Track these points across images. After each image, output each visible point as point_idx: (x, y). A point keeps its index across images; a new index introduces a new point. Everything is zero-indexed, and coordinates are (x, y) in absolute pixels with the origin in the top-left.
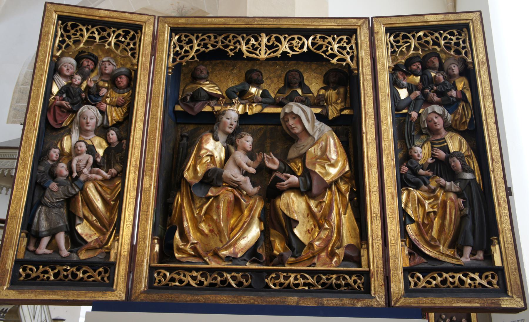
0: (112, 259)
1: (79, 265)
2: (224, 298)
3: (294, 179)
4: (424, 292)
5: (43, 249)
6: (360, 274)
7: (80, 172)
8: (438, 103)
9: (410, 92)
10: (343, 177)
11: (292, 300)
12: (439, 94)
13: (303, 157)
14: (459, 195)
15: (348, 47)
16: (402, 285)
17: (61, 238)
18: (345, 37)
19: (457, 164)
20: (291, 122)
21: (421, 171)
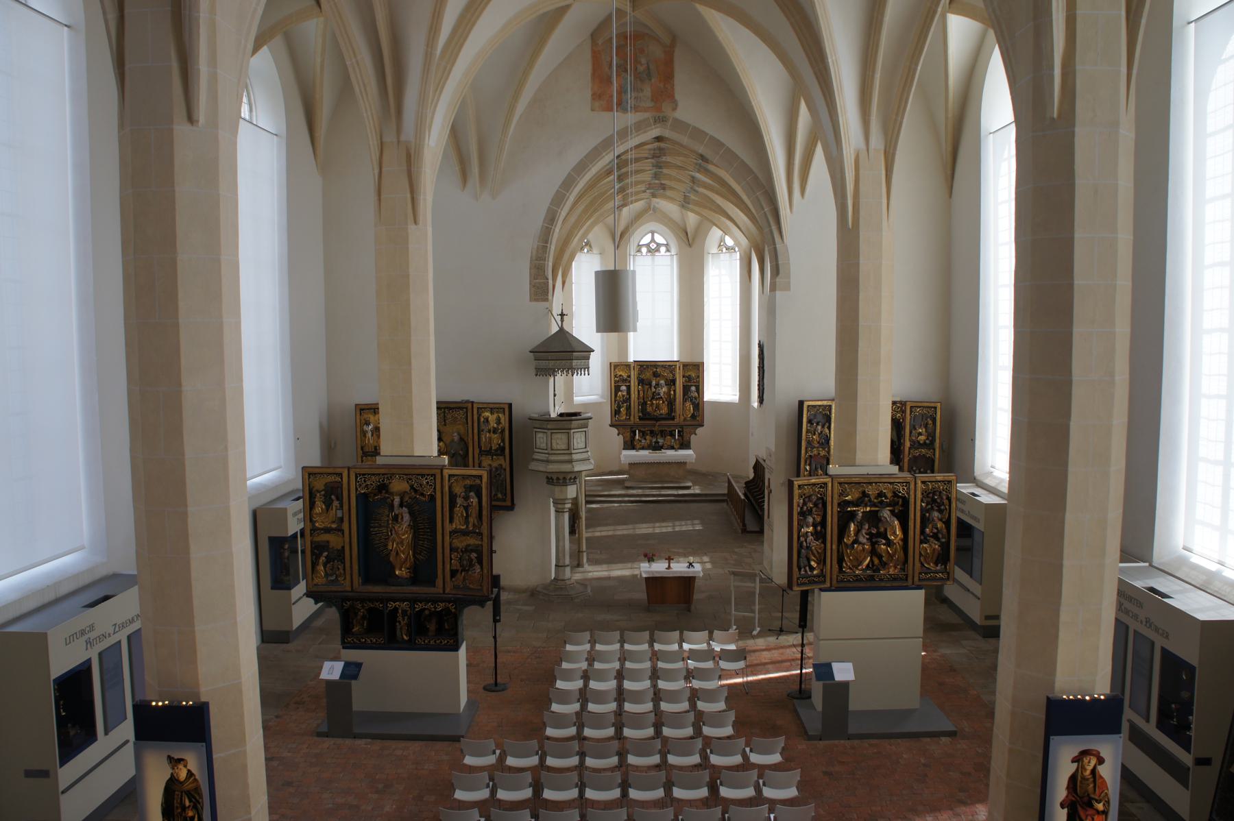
0: (824, 573)
1: (815, 576)
2: (862, 585)
3: (884, 541)
4: (924, 580)
5: (803, 572)
6: (905, 575)
7: (810, 544)
8: (937, 510)
9: (927, 505)
10: (902, 540)
11: (883, 584)
12: (937, 507)
13: (886, 530)
14: (939, 546)
15: (905, 488)
16: (918, 578)
17: (807, 568)
18: (904, 484)
19: (940, 536)
20: (883, 518)
21: (928, 538)
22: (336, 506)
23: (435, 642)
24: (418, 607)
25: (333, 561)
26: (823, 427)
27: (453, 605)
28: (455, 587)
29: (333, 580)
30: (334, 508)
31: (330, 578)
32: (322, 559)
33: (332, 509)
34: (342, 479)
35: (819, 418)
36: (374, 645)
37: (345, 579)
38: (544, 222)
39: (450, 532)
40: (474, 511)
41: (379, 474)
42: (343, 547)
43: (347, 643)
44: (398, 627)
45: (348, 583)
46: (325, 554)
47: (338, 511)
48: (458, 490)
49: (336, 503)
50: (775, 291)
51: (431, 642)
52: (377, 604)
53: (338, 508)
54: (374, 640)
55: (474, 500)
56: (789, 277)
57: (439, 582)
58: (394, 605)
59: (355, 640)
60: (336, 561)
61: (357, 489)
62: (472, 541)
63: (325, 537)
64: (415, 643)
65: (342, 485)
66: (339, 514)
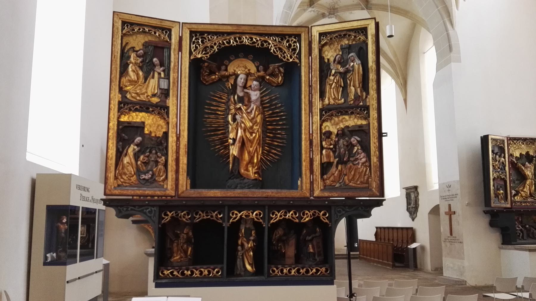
22: (159, 74)
23: (298, 271)
24: (277, 216)
25: (150, 152)
26: (500, 156)
27: (324, 215)
28: (326, 188)
29: (148, 180)
30: (156, 75)
31: (144, 176)
32: (132, 149)
33: (153, 77)
34: (170, 36)
35: (496, 150)
36: (206, 280)
37: (166, 178)
38: (284, 8)
39: (321, 110)
40: (356, 78)
41: (222, 34)
42: (166, 134)
43: (162, 278)
44: (240, 254)
45: (170, 184)
46: (138, 139)
47: (161, 80)
48: (330, 54)
49: (159, 69)
50: (450, 62)
51: (293, 271)
52: (214, 215)
53: (162, 75)
54: (206, 272)
55: (356, 64)
56: (459, 52)
57: (304, 182)
58: (239, 215)
59: (175, 273)
60: (154, 152)
61: (191, 53)
62: (351, 121)
63: (137, 117)
64: (269, 275)
65: (170, 44)
66: (164, 84)
